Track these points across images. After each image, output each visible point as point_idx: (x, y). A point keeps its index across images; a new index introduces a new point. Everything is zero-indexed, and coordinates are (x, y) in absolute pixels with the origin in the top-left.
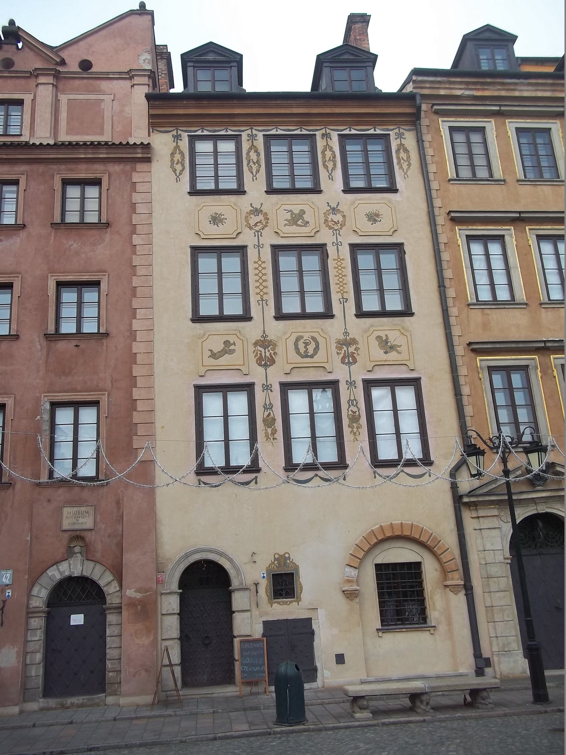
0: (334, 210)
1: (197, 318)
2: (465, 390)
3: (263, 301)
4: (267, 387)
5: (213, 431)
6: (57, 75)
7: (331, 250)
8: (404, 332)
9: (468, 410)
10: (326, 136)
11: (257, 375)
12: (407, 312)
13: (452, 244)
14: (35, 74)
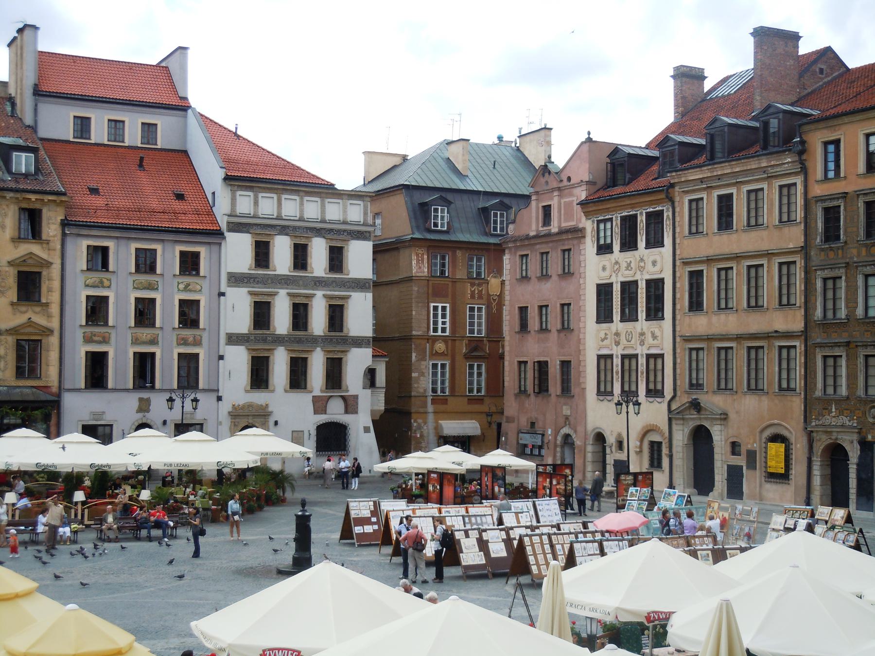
2: (678, 361)
6: (559, 189)
7: (639, 283)
9: (678, 371)
10: (641, 214)
14: (553, 190)
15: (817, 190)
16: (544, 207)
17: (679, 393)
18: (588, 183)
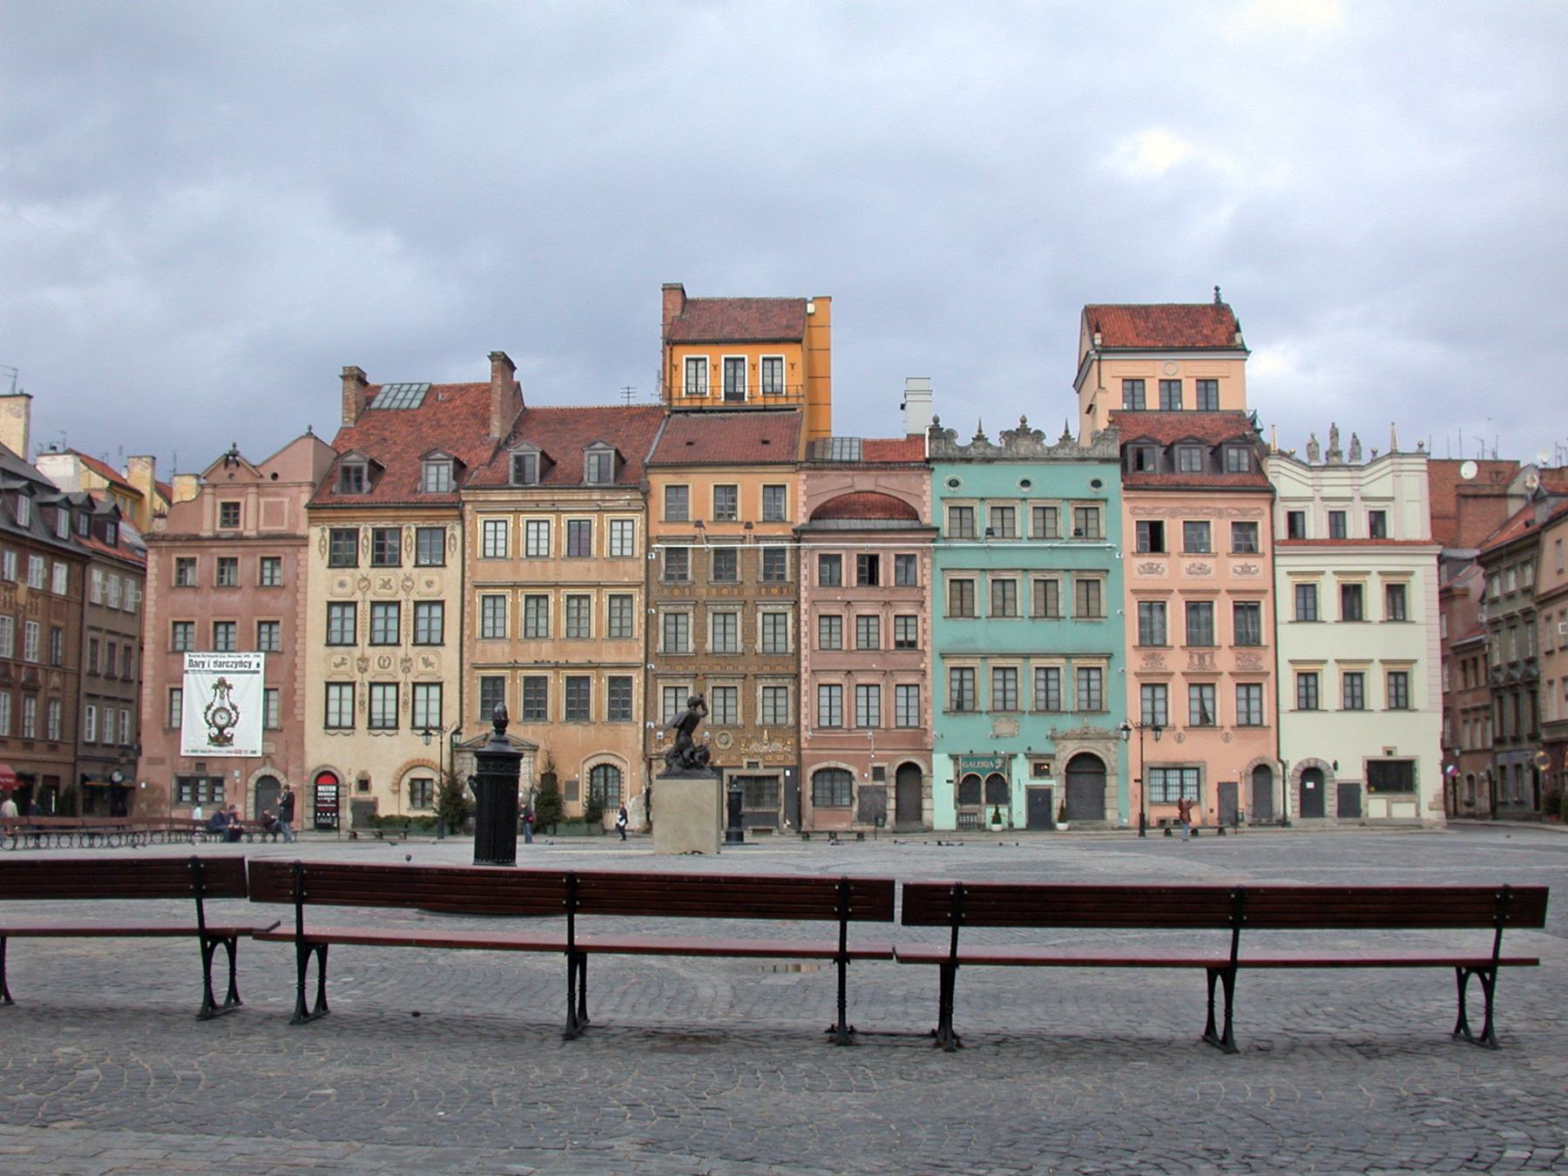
0: (408, 579)
1: (329, 644)
2: (466, 690)
3: (364, 635)
4: (362, 684)
5: (334, 706)
6: (258, 486)
8: (438, 655)
10: (409, 528)
11: (357, 677)
12: (442, 644)
13: (472, 601)
14: (246, 485)
15: (663, 531)
16: (225, 506)
17: (465, 725)
18: (313, 485)
